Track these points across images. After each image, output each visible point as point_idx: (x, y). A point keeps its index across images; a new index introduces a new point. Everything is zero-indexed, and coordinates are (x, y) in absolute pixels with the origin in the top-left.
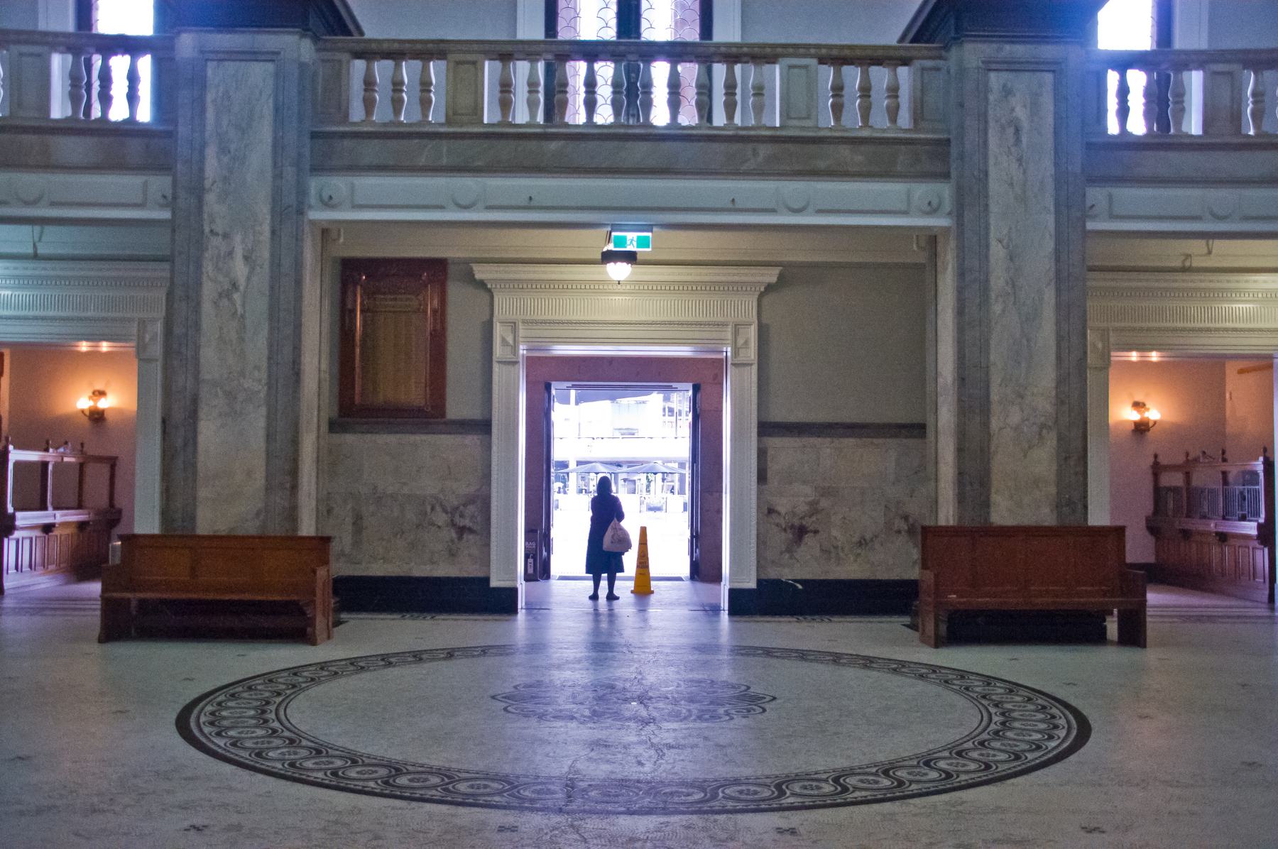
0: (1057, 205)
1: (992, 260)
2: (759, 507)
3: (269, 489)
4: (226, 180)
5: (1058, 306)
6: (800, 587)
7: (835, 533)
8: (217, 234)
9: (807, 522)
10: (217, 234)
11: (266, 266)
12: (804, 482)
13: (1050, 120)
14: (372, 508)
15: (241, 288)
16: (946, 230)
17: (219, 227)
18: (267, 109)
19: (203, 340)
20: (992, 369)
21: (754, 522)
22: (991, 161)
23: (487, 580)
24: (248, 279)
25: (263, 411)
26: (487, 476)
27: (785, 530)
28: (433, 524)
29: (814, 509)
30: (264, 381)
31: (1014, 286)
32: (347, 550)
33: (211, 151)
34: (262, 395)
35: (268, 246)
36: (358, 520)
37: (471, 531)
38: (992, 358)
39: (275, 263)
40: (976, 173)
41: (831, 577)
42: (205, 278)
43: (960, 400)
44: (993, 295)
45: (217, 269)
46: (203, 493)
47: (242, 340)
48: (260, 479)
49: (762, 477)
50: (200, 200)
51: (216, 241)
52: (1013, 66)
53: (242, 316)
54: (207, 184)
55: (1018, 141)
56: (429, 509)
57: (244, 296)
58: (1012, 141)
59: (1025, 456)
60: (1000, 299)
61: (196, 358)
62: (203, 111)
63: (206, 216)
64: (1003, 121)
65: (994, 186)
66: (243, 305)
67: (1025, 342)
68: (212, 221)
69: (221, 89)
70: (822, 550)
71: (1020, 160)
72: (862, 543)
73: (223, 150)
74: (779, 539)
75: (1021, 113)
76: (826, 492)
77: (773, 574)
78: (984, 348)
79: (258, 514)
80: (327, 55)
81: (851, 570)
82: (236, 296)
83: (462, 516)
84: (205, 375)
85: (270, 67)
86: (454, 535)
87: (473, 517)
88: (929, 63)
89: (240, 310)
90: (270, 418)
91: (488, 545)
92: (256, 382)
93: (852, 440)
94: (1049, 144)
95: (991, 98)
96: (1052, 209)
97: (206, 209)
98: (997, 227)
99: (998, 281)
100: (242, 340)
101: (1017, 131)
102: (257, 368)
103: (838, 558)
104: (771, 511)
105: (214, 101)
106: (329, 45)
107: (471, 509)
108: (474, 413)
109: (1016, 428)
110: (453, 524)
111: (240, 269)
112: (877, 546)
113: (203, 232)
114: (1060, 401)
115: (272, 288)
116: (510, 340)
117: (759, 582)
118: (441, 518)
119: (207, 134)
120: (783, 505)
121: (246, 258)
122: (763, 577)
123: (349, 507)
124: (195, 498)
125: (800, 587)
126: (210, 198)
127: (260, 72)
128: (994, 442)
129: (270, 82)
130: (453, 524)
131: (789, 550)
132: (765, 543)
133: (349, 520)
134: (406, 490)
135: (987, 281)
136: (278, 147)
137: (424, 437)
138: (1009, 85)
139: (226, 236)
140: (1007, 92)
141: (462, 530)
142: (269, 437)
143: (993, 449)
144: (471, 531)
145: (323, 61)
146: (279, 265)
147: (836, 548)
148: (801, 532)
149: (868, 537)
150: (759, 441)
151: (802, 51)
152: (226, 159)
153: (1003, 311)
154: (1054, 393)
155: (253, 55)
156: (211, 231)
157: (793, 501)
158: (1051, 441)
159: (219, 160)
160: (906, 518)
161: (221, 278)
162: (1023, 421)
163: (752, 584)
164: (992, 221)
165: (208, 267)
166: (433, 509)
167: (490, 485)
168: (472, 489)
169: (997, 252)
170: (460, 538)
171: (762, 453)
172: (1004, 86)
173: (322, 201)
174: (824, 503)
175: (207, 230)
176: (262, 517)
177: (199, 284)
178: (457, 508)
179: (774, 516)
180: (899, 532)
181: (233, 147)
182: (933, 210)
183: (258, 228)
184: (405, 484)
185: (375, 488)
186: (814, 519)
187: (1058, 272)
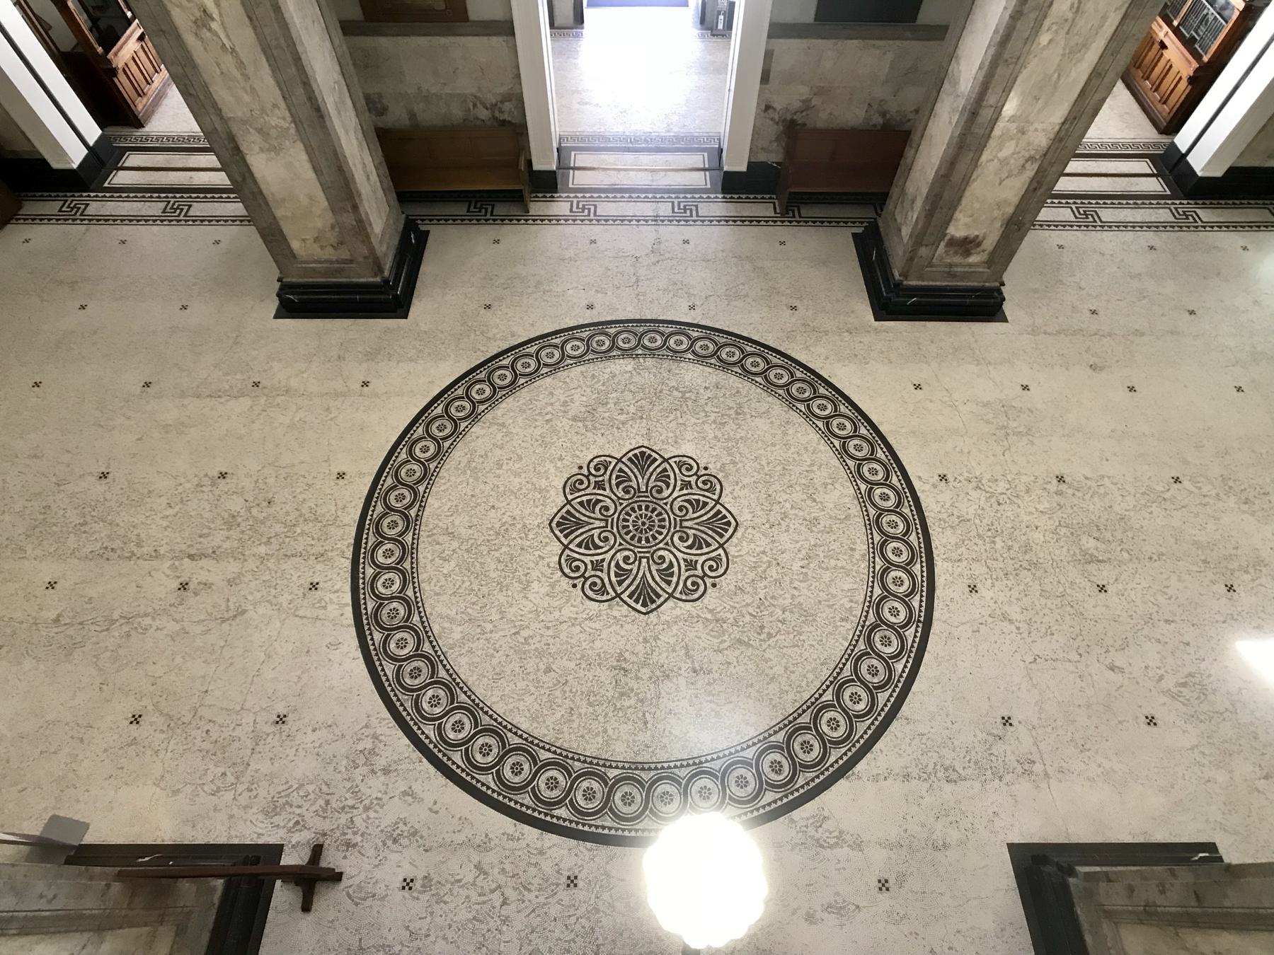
12: (802, 83)
14: (422, 105)
25: (300, 146)
26: (518, 76)
30: (289, 119)
47: (246, 77)
49: (765, 78)
53: (233, 50)
60: (1055, 27)
61: (209, 95)
66: (228, 36)
76: (819, 92)
77: (762, 157)
79: (333, 227)
82: (214, 25)
83: (501, 112)
84: (227, 113)
87: (510, 112)
89: (225, 41)
90: (309, 150)
92: (279, 118)
93: (855, 42)
100: (246, 77)
102: (275, 106)
107: (508, 106)
108: (496, 14)
115: (250, 18)
117: (750, 165)
124: (275, 218)
137: (452, 39)
142: (316, 170)
163: (743, 168)
166: (475, 105)
168: (504, 89)
171: (769, 55)
179: (770, 111)
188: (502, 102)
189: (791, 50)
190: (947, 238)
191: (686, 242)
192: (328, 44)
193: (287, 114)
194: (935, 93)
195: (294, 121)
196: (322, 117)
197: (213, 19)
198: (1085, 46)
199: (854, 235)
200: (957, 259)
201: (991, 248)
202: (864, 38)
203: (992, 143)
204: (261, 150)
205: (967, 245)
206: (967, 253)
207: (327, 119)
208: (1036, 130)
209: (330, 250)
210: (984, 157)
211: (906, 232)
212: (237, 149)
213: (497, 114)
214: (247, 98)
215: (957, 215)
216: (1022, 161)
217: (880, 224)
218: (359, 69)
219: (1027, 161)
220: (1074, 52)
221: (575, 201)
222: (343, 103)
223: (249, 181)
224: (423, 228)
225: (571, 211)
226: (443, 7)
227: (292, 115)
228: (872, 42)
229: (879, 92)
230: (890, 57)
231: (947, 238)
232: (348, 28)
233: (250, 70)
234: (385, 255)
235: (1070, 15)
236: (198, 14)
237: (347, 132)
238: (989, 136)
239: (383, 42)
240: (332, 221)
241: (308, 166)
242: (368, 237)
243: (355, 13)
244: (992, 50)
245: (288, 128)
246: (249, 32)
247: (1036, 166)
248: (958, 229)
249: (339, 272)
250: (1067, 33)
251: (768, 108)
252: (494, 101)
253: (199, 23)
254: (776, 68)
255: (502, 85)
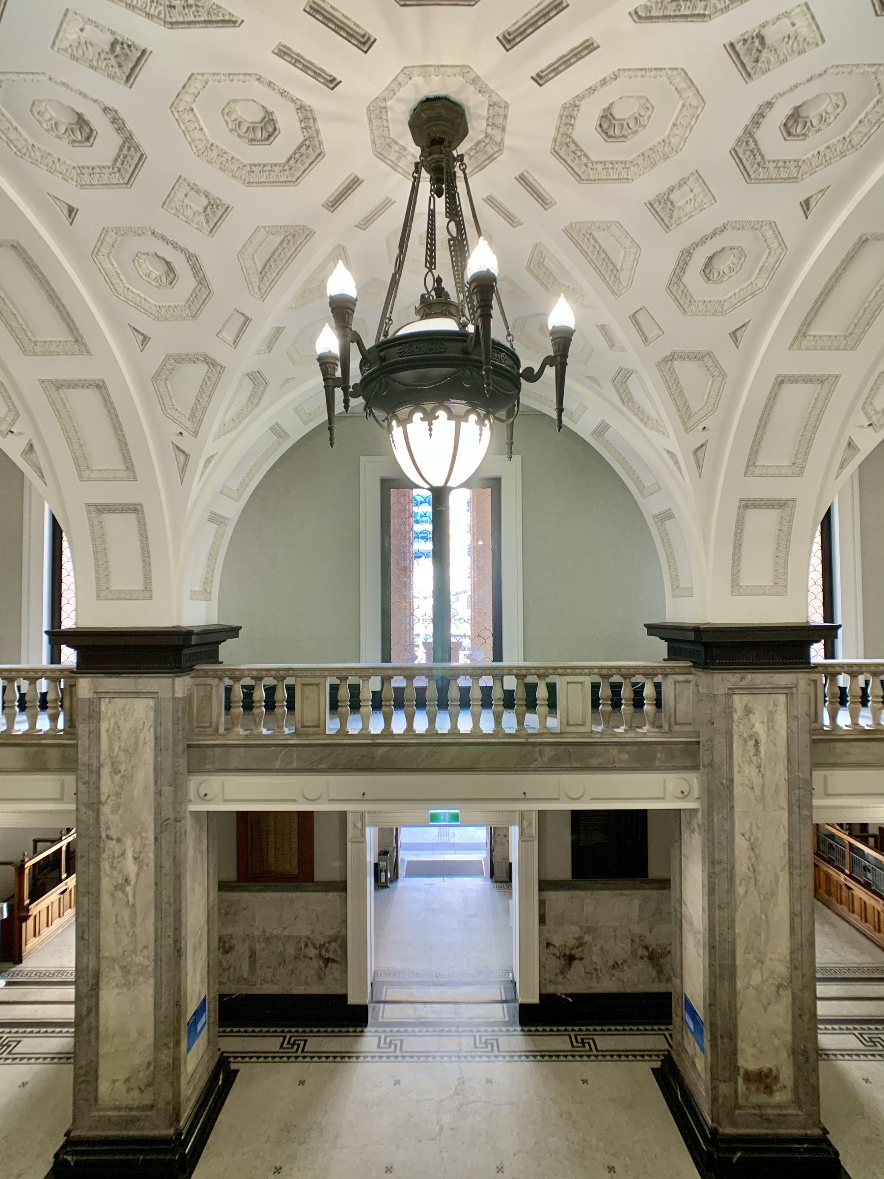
0: (790, 805)
1: (737, 853)
2: (540, 942)
3: (157, 1047)
4: (118, 795)
5: (791, 889)
6: (570, 1000)
7: (595, 959)
8: (112, 839)
9: (576, 952)
10: (112, 839)
11: (152, 864)
13: (783, 733)
14: (263, 945)
15: (132, 883)
16: (694, 811)
17: (114, 833)
18: (148, 736)
19: (103, 924)
20: (738, 941)
21: (537, 953)
22: (736, 769)
23: (345, 997)
24: (138, 875)
25: (152, 981)
26: (345, 922)
27: (559, 958)
28: (306, 957)
29: (580, 943)
30: (152, 958)
31: (754, 871)
32: (246, 975)
33: (106, 772)
34: (151, 968)
35: (152, 847)
36: (253, 955)
37: (333, 961)
38: (737, 931)
39: (159, 867)
40: (724, 781)
41: (593, 991)
42: (102, 873)
43: (711, 965)
44: (737, 881)
45: (113, 867)
46: (105, 1048)
47: (133, 925)
48: (150, 1039)
49: (542, 920)
50: (98, 812)
51: (112, 844)
52: (752, 690)
53: (133, 905)
54: (103, 798)
55: (757, 752)
56: (303, 946)
57: (135, 889)
58: (752, 751)
59: (765, 1010)
62: (99, 738)
63: (102, 824)
64: (745, 735)
65: (738, 790)
66: (134, 898)
67: (763, 917)
68: (108, 828)
69: (112, 720)
70: (586, 973)
71: (759, 767)
72: (615, 966)
73: (116, 771)
74: (555, 964)
75: (760, 728)
76: (589, 930)
77: (551, 989)
78: (731, 926)
79: (149, 1065)
80: (199, 681)
81: (607, 985)
83: (327, 950)
84: (105, 953)
85: (151, 702)
86: (321, 963)
87: (335, 951)
88: (681, 678)
89: (131, 899)
91: (346, 971)
92: (145, 959)
93: (607, 892)
94: (784, 753)
95: (735, 717)
96: (786, 807)
97: (102, 817)
98: (741, 824)
99: (742, 868)
100: (133, 925)
101: (757, 742)
102: (145, 947)
103: (598, 978)
104: (548, 945)
105: (108, 731)
106: (201, 673)
107: (333, 946)
109: (758, 988)
110: (321, 957)
111: (131, 868)
112: (626, 968)
113: (100, 837)
114: (794, 966)
115: (156, 884)
116: (359, 825)
117: (542, 996)
118: (312, 952)
119: (102, 758)
120: (557, 940)
121: (135, 858)
122: (544, 992)
123: (246, 944)
125: (570, 1000)
126: (106, 810)
127: (142, 708)
128: (740, 999)
129: (152, 714)
130: (321, 957)
131: (562, 972)
132: (545, 968)
133: (247, 954)
134: (287, 933)
135: (733, 868)
136: (158, 770)
137: (299, 894)
138: (750, 705)
139: (119, 840)
140: (748, 711)
141: (327, 961)
142: (157, 1005)
143: (738, 1005)
144: (333, 961)
145: (197, 685)
146: (161, 867)
147: (596, 970)
148: (571, 959)
149: (619, 962)
150: (539, 895)
151: (578, 671)
152: (117, 778)
153: (746, 892)
154: (788, 958)
155: (138, 694)
156: (108, 836)
157: (565, 936)
158: (786, 997)
159: (112, 779)
160: (646, 948)
161: (115, 874)
162: (763, 982)
163: (536, 1000)
164: (737, 819)
165: (106, 866)
166: (306, 946)
167: (346, 928)
168: (333, 932)
169: (741, 843)
170: (326, 966)
171: (542, 903)
172: (746, 706)
173: (200, 797)
174: (587, 938)
175: (104, 835)
176: (152, 1068)
177: (98, 879)
178: (324, 945)
179: (551, 947)
180: (642, 958)
181: (123, 767)
182: (684, 796)
183: (144, 834)
184: (285, 928)
185: (264, 932)
186: (580, 949)
187: (791, 860)
188: (329, 943)
189: (558, 899)
190: (742, 1072)
191: (489, 1081)
192: (204, 900)
193: (153, 954)
194: (678, 931)
195: (155, 961)
196: (180, 957)
197: (129, 884)
198: (773, 894)
199: (654, 1070)
200: (763, 1098)
201: (790, 1084)
202: (613, 889)
203: (740, 972)
204: (117, 986)
205: (764, 1080)
206: (769, 1090)
207: (183, 958)
208: (771, 959)
209: (135, 1093)
210: (740, 984)
211: (700, 1064)
212: (96, 986)
213: (324, 953)
214: (126, 940)
215: (740, 1044)
216: (773, 988)
217: (675, 1056)
218: (222, 912)
219: (779, 988)
220: (769, 897)
221: (383, 1035)
222: (200, 943)
223: (93, 1014)
224: (233, 1066)
225: (379, 1046)
226: (297, 872)
227: (156, 955)
228: (618, 892)
229: (637, 930)
230: (636, 902)
231: (742, 1072)
232: (223, 886)
233: (139, 919)
234: (188, 1099)
235: (751, 874)
236: (120, 881)
237: (195, 969)
238: (734, 967)
239: (246, 896)
240: (151, 1058)
241: (150, 1001)
242: (178, 1077)
243: (232, 875)
244: (706, 898)
245: (148, 966)
246: (151, 895)
247: (789, 992)
248: (748, 1061)
249: (134, 1121)
250: (756, 885)
251: (548, 945)
252: (323, 941)
253: (118, 887)
254: (549, 914)
255: (332, 928)
